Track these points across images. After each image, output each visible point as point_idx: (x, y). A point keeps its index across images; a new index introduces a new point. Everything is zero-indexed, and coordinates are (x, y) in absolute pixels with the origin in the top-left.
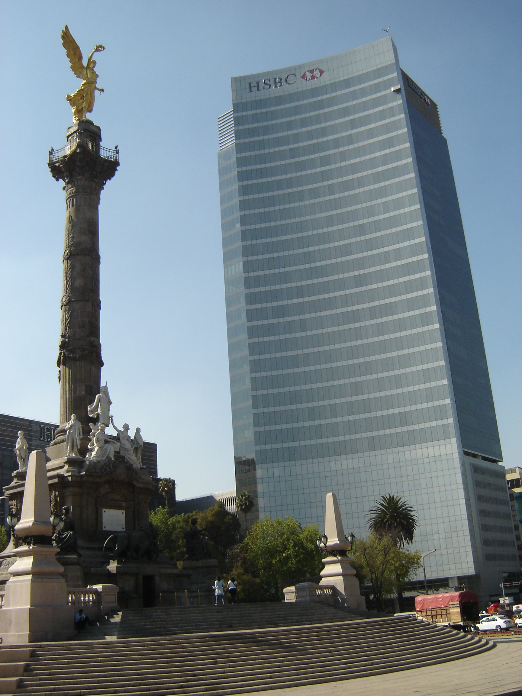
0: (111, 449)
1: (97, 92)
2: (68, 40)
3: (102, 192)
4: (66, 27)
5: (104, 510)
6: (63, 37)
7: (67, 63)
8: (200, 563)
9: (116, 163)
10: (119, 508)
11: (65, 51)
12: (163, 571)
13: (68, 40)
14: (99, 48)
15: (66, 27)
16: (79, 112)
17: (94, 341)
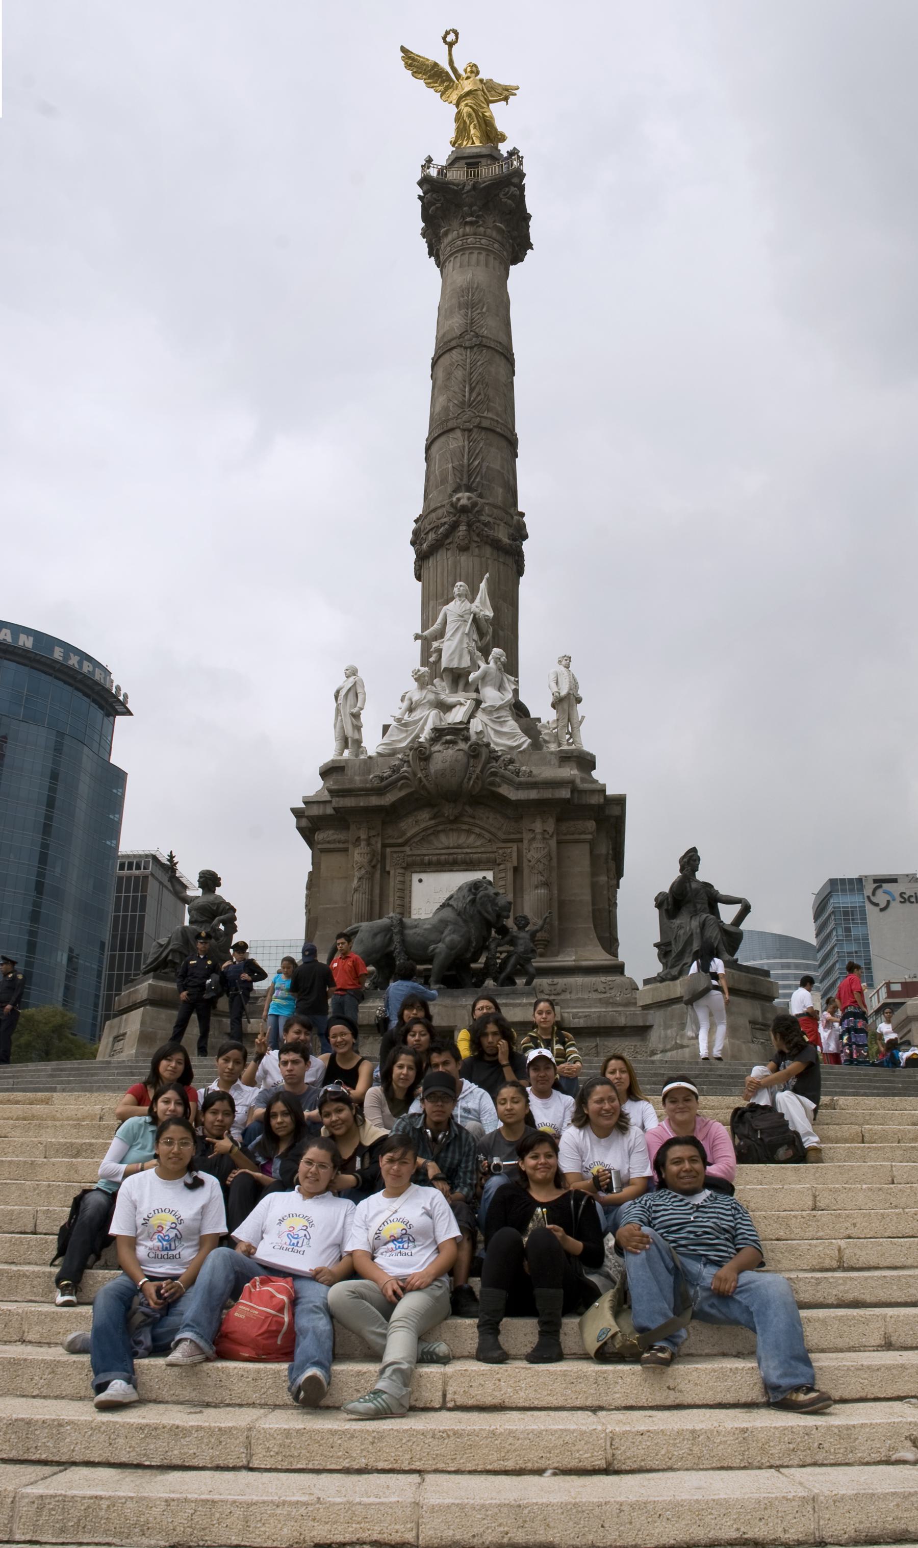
0: (430, 719)
5: (415, 877)
17: (459, 499)
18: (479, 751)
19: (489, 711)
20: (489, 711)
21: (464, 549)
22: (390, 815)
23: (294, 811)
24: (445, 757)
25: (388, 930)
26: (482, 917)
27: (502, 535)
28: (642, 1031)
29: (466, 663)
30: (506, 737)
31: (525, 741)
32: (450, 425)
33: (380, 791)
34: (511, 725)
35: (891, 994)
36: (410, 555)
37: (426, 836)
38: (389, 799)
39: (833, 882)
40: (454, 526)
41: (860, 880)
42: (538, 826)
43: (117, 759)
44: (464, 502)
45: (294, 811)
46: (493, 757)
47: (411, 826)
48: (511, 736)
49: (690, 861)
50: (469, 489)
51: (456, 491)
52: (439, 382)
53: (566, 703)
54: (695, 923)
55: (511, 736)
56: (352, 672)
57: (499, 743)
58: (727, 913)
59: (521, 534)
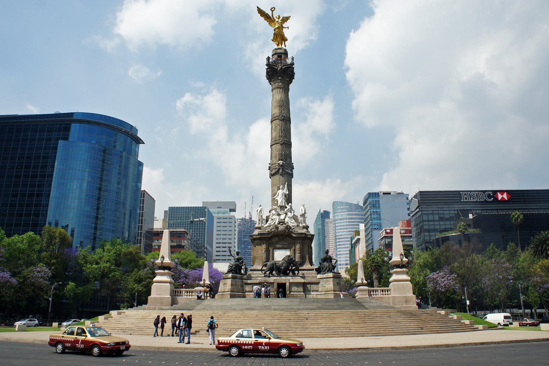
0: (277, 219)
1: (284, 30)
2: (261, 12)
4: (258, 7)
8: (325, 276)
9: (293, 64)
10: (285, 249)
12: (291, 281)
13: (261, 12)
14: (273, 10)
15: (258, 7)
16: (278, 45)
18: (288, 228)
19: (289, 217)
20: (289, 217)
24: (281, 227)
25: (273, 264)
26: (290, 261)
28: (318, 283)
29: (283, 204)
30: (292, 223)
31: (295, 224)
32: (278, 142)
34: (293, 221)
35: (387, 233)
36: (268, 172)
37: (277, 243)
39: (369, 194)
40: (279, 169)
41: (378, 193)
42: (298, 241)
43: (140, 159)
44: (281, 164)
46: (290, 228)
47: (274, 240)
48: (293, 223)
49: (327, 252)
50: (282, 160)
51: (279, 160)
53: (303, 215)
54: (328, 264)
55: (293, 223)
57: (291, 225)
58: (334, 262)
59: (292, 168)
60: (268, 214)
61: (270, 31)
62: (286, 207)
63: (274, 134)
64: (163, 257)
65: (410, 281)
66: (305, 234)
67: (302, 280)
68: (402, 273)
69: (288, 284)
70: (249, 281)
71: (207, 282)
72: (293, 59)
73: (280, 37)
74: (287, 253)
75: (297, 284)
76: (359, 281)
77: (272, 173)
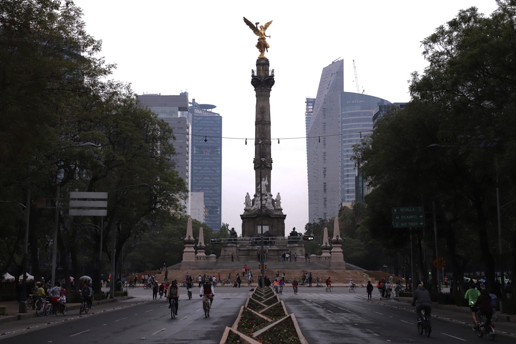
1: (267, 40)
3: (273, 88)
4: (244, 18)
6: (245, 22)
7: (252, 31)
8: (292, 245)
9: (273, 76)
11: (248, 27)
12: (269, 249)
14: (257, 24)
15: (244, 18)
21: (263, 169)
22: (256, 217)
23: (241, 215)
26: (268, 234)
27: (269, 166)
30: (271, 207)
31: (273, 208)
33: (254, 215)
34: (272, 205)
38: (255, 216)
45: (241, 215)
49: (294, 229)
50: (264, 157)
52: (257, 130)
56: (248, 193)
60: (253, 198)
61: (256, 38)
62: (266, 195)
63: (258, 136)
64: (189, 237)
65: (343, 252)
66: (279, 215)
67: (277, 249)
68: (338, 247)
69: (267, 251)
70: (241, 249)
71: (203, 244)
72: (273, 71)
73: (262, 46)
74: (266, 228)
75: (274, 251)
76: (324, 245)
77: (257, 166)
